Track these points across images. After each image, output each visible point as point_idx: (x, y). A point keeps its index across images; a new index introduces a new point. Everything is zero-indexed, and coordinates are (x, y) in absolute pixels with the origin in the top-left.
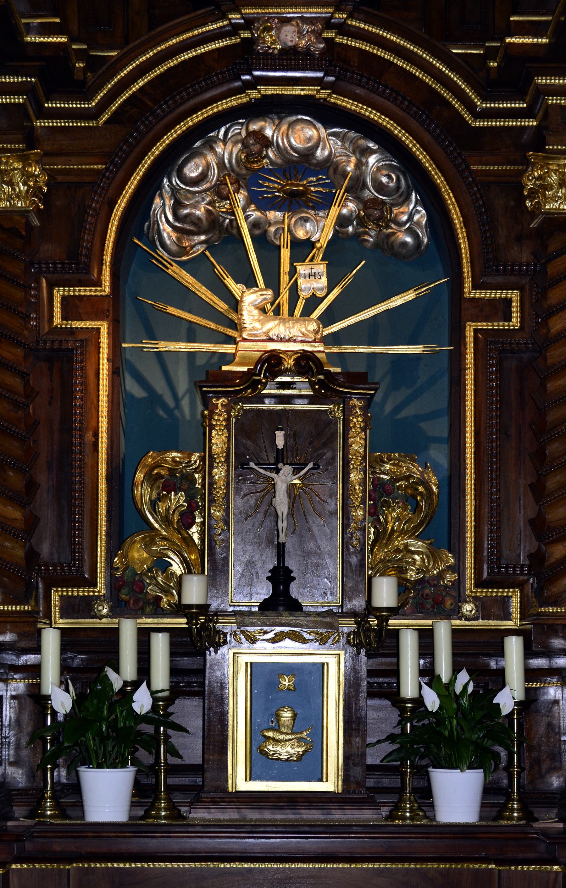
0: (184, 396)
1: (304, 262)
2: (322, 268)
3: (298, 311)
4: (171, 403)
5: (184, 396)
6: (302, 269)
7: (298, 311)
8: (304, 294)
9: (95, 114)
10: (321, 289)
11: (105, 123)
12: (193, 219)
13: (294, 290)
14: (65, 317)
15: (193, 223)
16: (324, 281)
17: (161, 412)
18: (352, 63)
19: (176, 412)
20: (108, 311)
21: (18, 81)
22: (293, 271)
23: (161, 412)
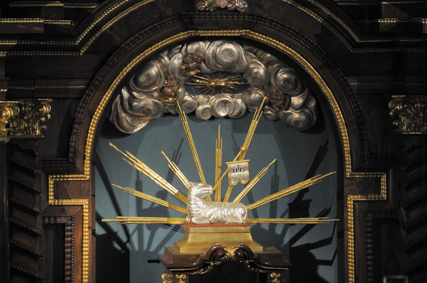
0: (133, 232)
1: (232, 161)
2: (244, 163)
3: (228, 195)
4: (124, 239)
5: (133, 232)
6: (232, 165)
7: (228, 195)
8: (233, 183)
9: (77, 49)
10: (244, 178)
11: (85, 53)
12: (144, 109)
13: (226, 181)
14: (56, 197)
15: (144, 112)
16: (247, 173)
17: (116, 246)
18: (264, 7)
19: (128, 245)
20: (88, 191)
21: (30, 44)
22: (224, 167)
23: (116, 246)
